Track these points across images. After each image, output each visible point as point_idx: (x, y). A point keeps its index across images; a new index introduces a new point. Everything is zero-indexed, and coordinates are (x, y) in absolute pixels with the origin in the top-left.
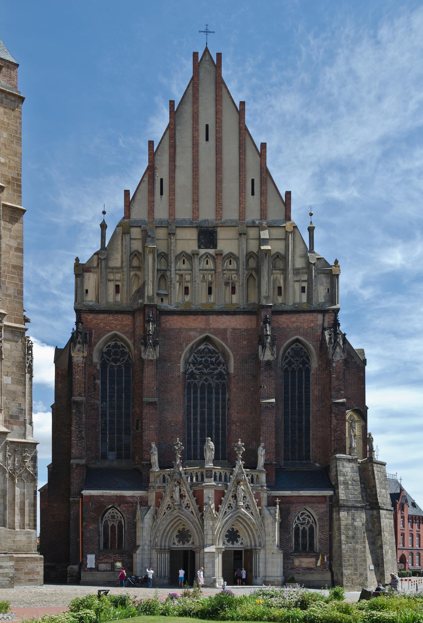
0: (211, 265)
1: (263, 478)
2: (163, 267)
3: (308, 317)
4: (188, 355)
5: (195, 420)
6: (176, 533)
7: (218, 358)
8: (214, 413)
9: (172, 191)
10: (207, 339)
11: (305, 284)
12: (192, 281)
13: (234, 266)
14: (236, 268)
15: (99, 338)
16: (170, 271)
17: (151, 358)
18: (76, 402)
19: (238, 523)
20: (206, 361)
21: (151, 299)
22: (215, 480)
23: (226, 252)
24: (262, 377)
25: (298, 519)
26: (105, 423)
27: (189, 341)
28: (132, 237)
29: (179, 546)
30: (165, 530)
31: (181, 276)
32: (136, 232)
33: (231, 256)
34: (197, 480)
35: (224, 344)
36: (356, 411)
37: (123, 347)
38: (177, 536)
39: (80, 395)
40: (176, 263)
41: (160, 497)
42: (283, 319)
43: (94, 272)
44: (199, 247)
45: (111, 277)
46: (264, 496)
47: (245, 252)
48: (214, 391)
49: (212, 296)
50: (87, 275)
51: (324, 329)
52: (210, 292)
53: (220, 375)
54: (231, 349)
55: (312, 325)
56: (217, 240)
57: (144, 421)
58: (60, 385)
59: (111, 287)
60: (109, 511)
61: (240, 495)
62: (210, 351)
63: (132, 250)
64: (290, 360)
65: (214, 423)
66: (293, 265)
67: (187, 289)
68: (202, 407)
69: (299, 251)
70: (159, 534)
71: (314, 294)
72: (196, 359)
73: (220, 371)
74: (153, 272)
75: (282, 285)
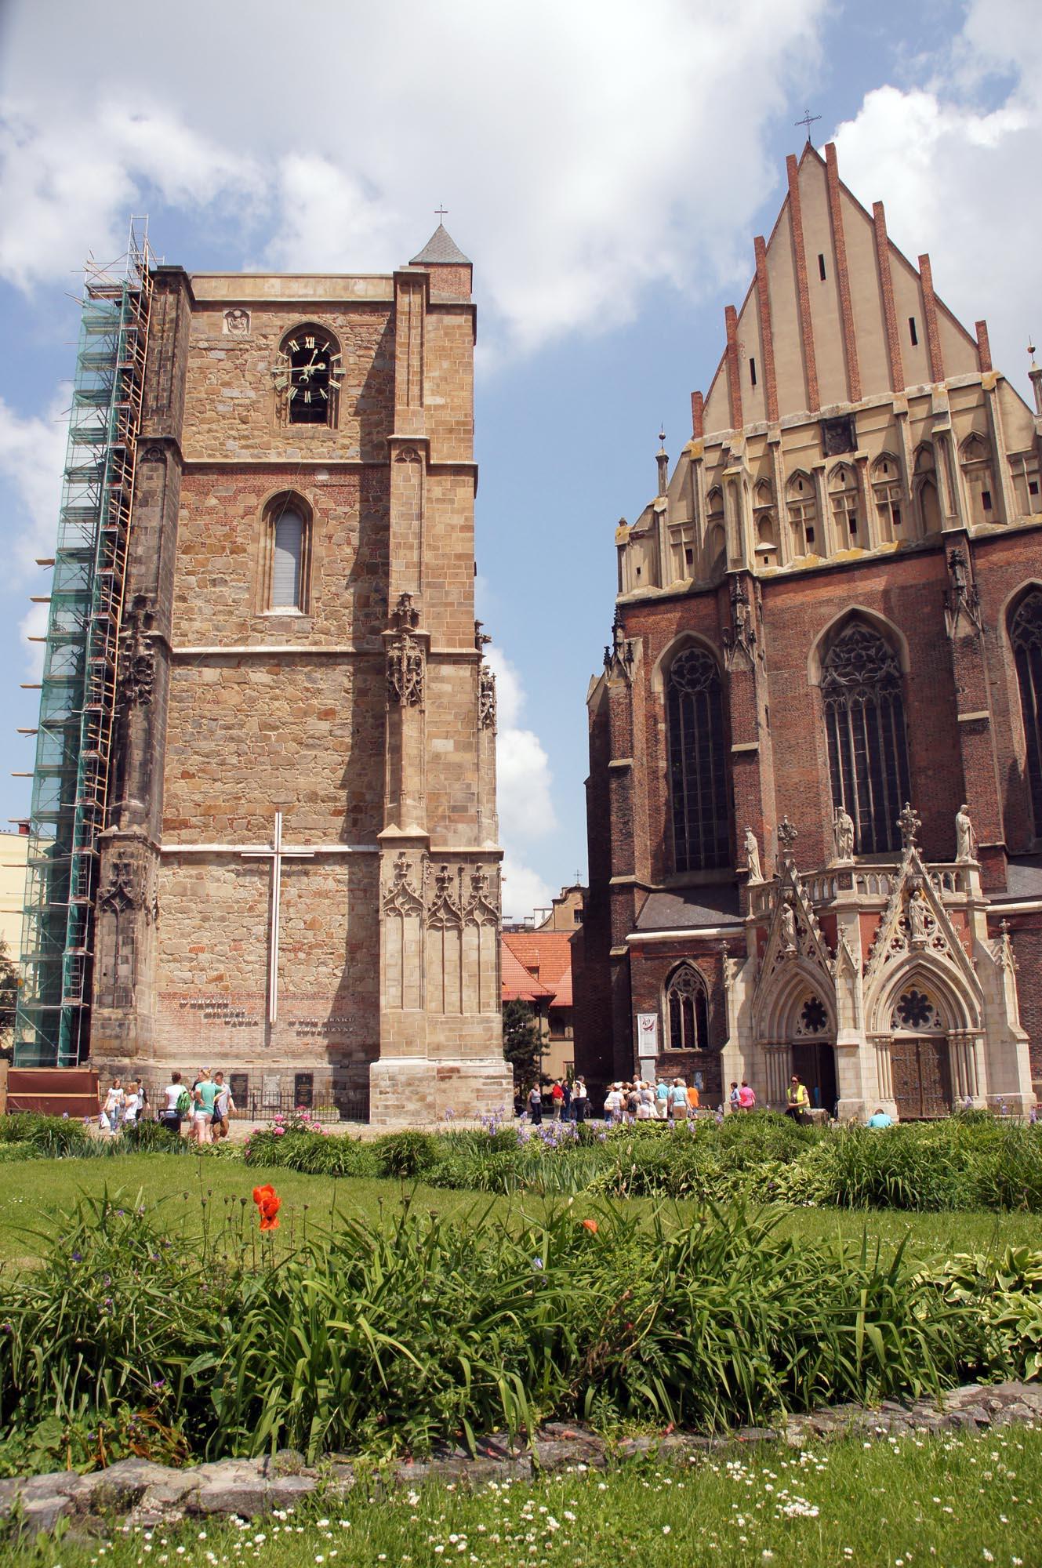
1: (974, 878)
6: (801, 1010)
7: (879, 649)
10: (854, 616)
12: (818, 516)
15: (659, 649)
16: (776, 506)
19: (920, 978)
27: (821, 625)
29: (806, 1035)
30: (776, 1003)
37: (704, 656)
38: (804, 1016)
39: (623, 756)
41: (763, 937)
42: (998, 556)
48: (879, 712)
49: (858, 534)
53: (889, 681)
56: (856, 435)
58: (598, 742)
60: (678, 972)
61: (916, 920)
62: (865, 638)
64: (1025, 629)
65: (884, 775)
69: (1017, 418)
70: (767, 1013)
72: (838, 656)
73: (888, 673)
75: (989, 488)
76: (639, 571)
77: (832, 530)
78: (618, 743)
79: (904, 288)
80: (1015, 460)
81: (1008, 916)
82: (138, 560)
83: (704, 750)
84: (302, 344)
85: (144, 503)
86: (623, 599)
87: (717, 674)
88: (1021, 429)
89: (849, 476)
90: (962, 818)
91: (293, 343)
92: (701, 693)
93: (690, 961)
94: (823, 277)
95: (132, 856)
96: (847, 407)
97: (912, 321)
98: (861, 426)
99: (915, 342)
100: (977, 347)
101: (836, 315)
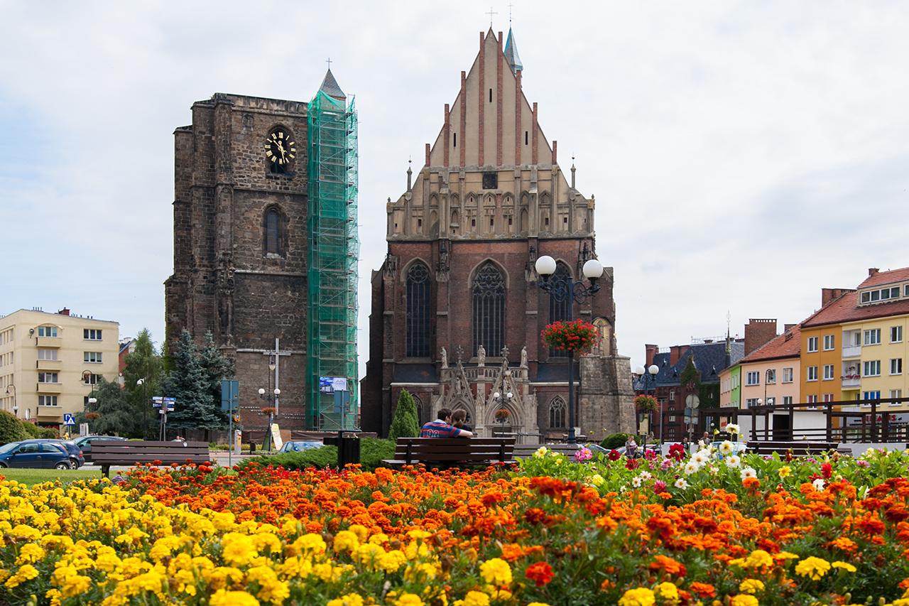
0: (493, 203)
1: (525, 373)
2: (456, 206)
3: (568, 243)
4: (474, 274)
5: (480, 325)
8: (495, 320)
9: (463, 143)
10: (489, 261)
11: (567, 216)
13: (510, 203)
14: (512, 204)
17: (443, 281)
18: (387, 315)
20: (489, 278)
21: (444, 234)
22: (486, 376)
23: (504, 192)
24: (528, 294)
25: (553, 403)
26: (410, 329)
27: (475, 264)
28: (432, 181)
31: (470, 210)
32: (434, 178)
33: (508, 194)
34: (473, 376)
35: (502, 266)
36: (605, 318)
39: (390, 310)
40: (465, 201)
41: (447, 388)
43: (402, 210)
44: (484, 188)
45: (415, 214)
46: (526, 387)
47: (519, 192)
49: (494, 227)
50: (396, 213)
51: (580, 252)
52: (492, 224)
53: (500, 290)
54: (507, 269)
55: (571, 249)
57: (438, 330)
58: (375, 300)
59: (415, 221)
63: (432, 191)
65: (495, 327)
66: (558, 201)
67: (474, 221)
68: (486, 314)
71: (573, 225)
74: (446, 211)
75: (549, 217)
76: (396, 225)
77: (484, 221)
78: (387, 304)
79: (526, 117)
80: (560, 207)
81: (536, 387)
82: (222, 236)
83: (421, 308)
84: (277, 136)
85: (223, 212)
86: (390, 238)
87: (429, 276)
88: (564, 194)
89: (492, 199)
90: (524, 352)
91: (274, 135)
92: (421, 284)
93: (416, 394)
94: (491, 101)
95: (233, 356)
96: (495, 167)
97: (527, 132)
98: (501, 177)
99: (527, 144)
100: (552, 152)
101: (496, 121)
